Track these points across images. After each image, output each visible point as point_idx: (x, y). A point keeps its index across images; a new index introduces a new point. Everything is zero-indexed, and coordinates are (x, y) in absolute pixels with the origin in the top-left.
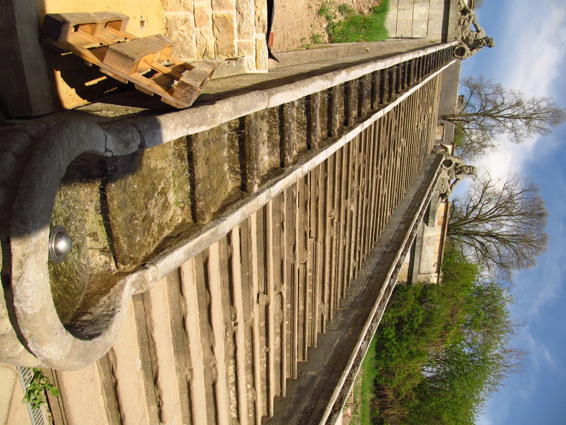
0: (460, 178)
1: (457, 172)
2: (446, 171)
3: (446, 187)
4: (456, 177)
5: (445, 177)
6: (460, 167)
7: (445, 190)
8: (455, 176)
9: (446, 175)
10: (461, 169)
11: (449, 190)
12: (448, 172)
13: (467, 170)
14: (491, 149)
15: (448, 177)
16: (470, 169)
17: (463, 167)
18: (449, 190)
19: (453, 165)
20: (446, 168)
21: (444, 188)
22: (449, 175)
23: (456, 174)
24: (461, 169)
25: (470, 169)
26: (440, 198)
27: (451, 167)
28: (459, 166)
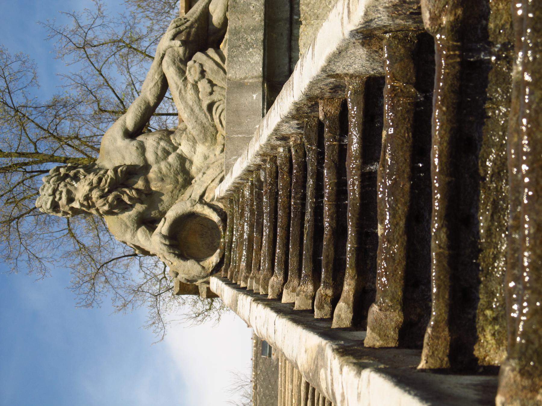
0: (122, 143)
1: (140, 184)
2: (195, 190)
3: (190, 94)
4: (142, 148)
5: (201, 149)
6: (124, 207)
7: (192, 74)
8: (150, 157)
9: (197, 160)
10: (118, 199)
11: (171, 74)
12: (188, 180)
13: (87, 198)
14: (90, 36)
15: (184, 148)
16: (71, 200)
17: (110, 213)
18: (171, 74)
19: (163, 227)
20: (199, 209)
21: (203, 85)
22: (182, 159)
23: (147, 167)
24: (118, 199)
25: (71, 200)
26: (216, 18)
27: (171, 215)
28: (133, 213)
